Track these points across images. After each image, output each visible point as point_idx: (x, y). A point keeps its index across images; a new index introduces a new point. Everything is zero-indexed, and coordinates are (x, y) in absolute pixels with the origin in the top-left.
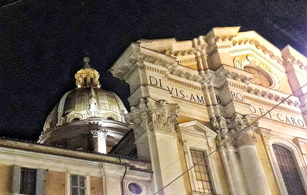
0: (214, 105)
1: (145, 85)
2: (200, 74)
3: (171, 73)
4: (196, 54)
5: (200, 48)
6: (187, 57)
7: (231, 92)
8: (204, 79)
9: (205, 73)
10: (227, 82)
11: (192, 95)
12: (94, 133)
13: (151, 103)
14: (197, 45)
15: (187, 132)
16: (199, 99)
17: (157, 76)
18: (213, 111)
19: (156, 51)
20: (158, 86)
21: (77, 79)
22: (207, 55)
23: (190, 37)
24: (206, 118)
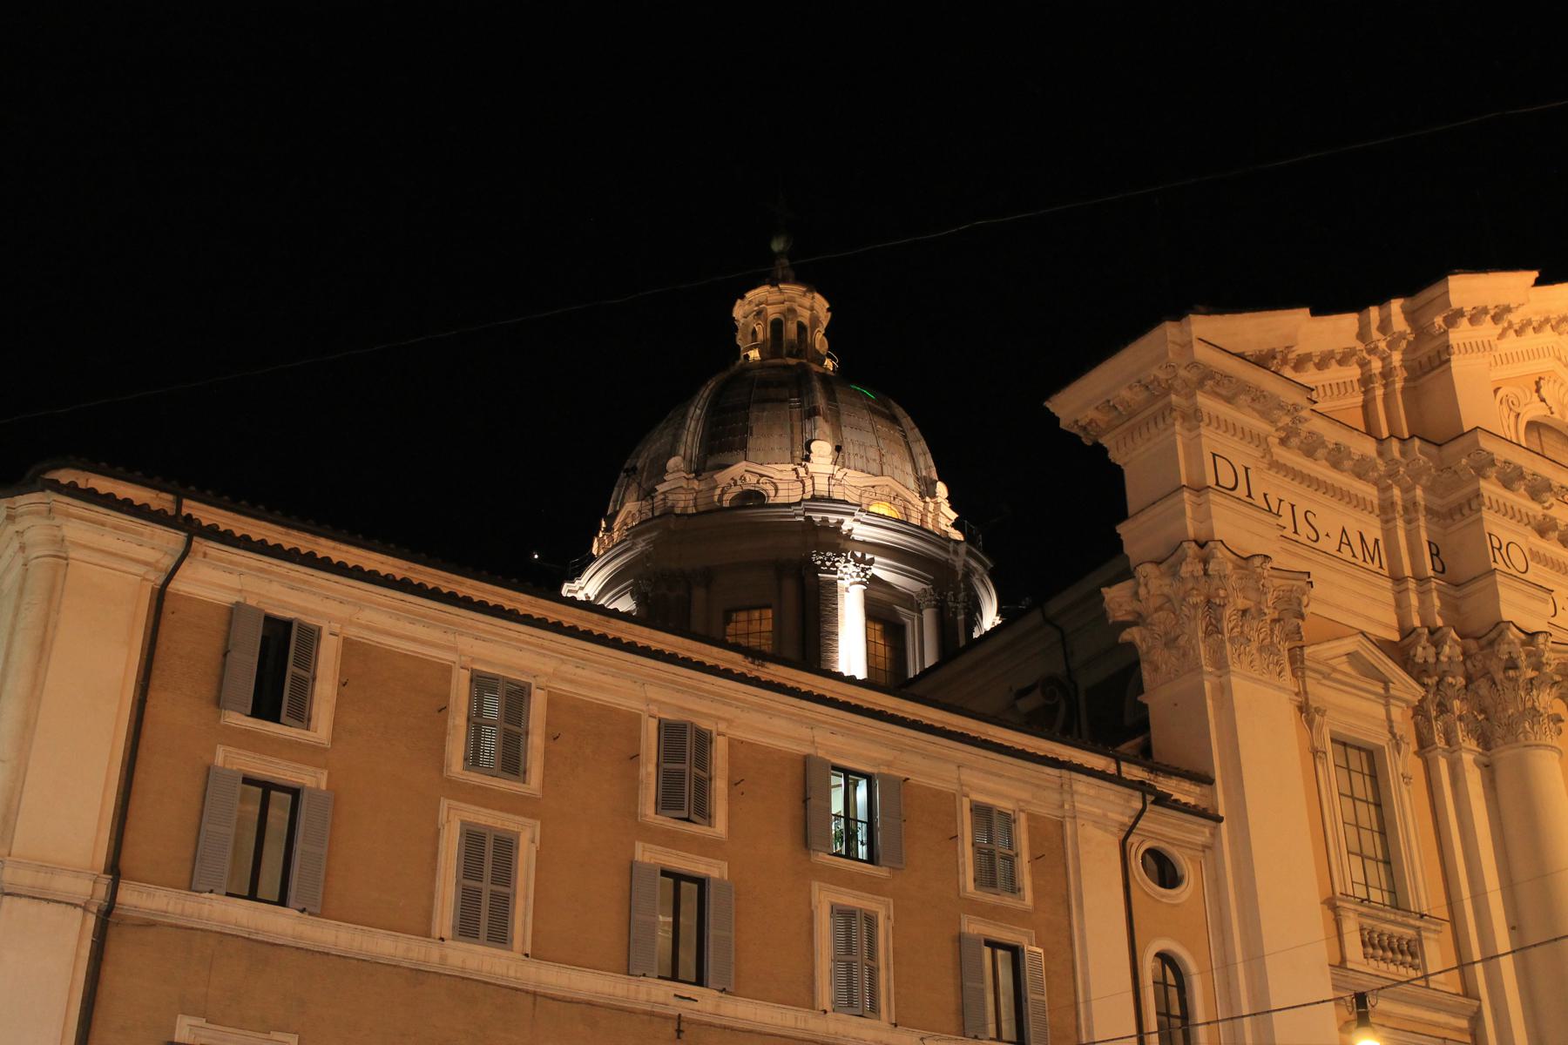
0: (1421, 580)
1: (1200, 489)
2: (1380, 454)
4: (1363, 364)
5: (1382, 345)
6: (1335, 373)
7: (1490, 535)
8: (1392, 474)
9: (1403, 454)
10: (1478, 494)
11: (1344, 530)
12: (823, 561)
13: (1222, 562)
14: (1376, 335)
15: (1326, 676)
16: (1365, 549)
17: (1239, 453)
18: (1414, 600)
19: (1241, 356)
20: (1239, 491)
21: (742, 321)
22: (1405, 375)
24: (1387, 626)
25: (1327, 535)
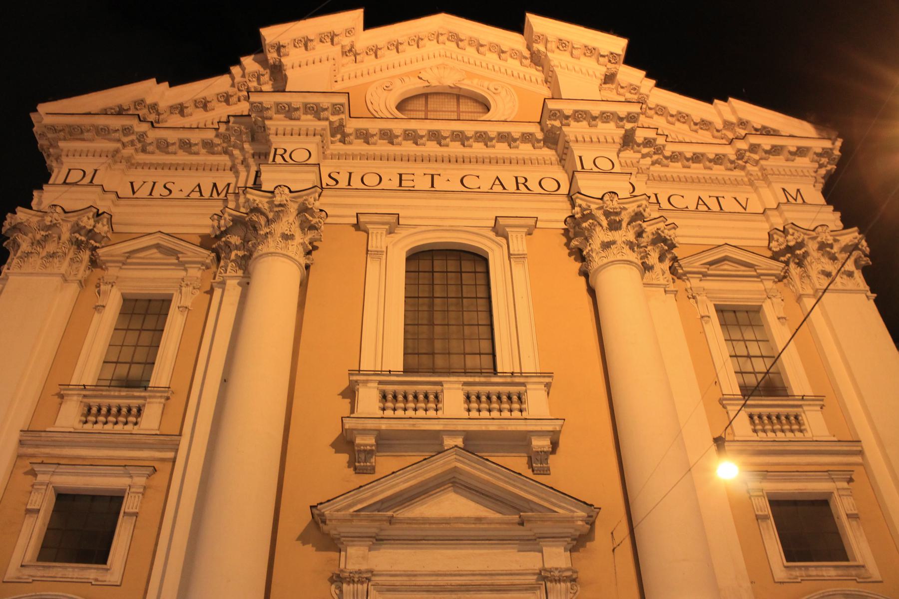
3: (144, 150)
23: (220, 68)
25: (181, 190)
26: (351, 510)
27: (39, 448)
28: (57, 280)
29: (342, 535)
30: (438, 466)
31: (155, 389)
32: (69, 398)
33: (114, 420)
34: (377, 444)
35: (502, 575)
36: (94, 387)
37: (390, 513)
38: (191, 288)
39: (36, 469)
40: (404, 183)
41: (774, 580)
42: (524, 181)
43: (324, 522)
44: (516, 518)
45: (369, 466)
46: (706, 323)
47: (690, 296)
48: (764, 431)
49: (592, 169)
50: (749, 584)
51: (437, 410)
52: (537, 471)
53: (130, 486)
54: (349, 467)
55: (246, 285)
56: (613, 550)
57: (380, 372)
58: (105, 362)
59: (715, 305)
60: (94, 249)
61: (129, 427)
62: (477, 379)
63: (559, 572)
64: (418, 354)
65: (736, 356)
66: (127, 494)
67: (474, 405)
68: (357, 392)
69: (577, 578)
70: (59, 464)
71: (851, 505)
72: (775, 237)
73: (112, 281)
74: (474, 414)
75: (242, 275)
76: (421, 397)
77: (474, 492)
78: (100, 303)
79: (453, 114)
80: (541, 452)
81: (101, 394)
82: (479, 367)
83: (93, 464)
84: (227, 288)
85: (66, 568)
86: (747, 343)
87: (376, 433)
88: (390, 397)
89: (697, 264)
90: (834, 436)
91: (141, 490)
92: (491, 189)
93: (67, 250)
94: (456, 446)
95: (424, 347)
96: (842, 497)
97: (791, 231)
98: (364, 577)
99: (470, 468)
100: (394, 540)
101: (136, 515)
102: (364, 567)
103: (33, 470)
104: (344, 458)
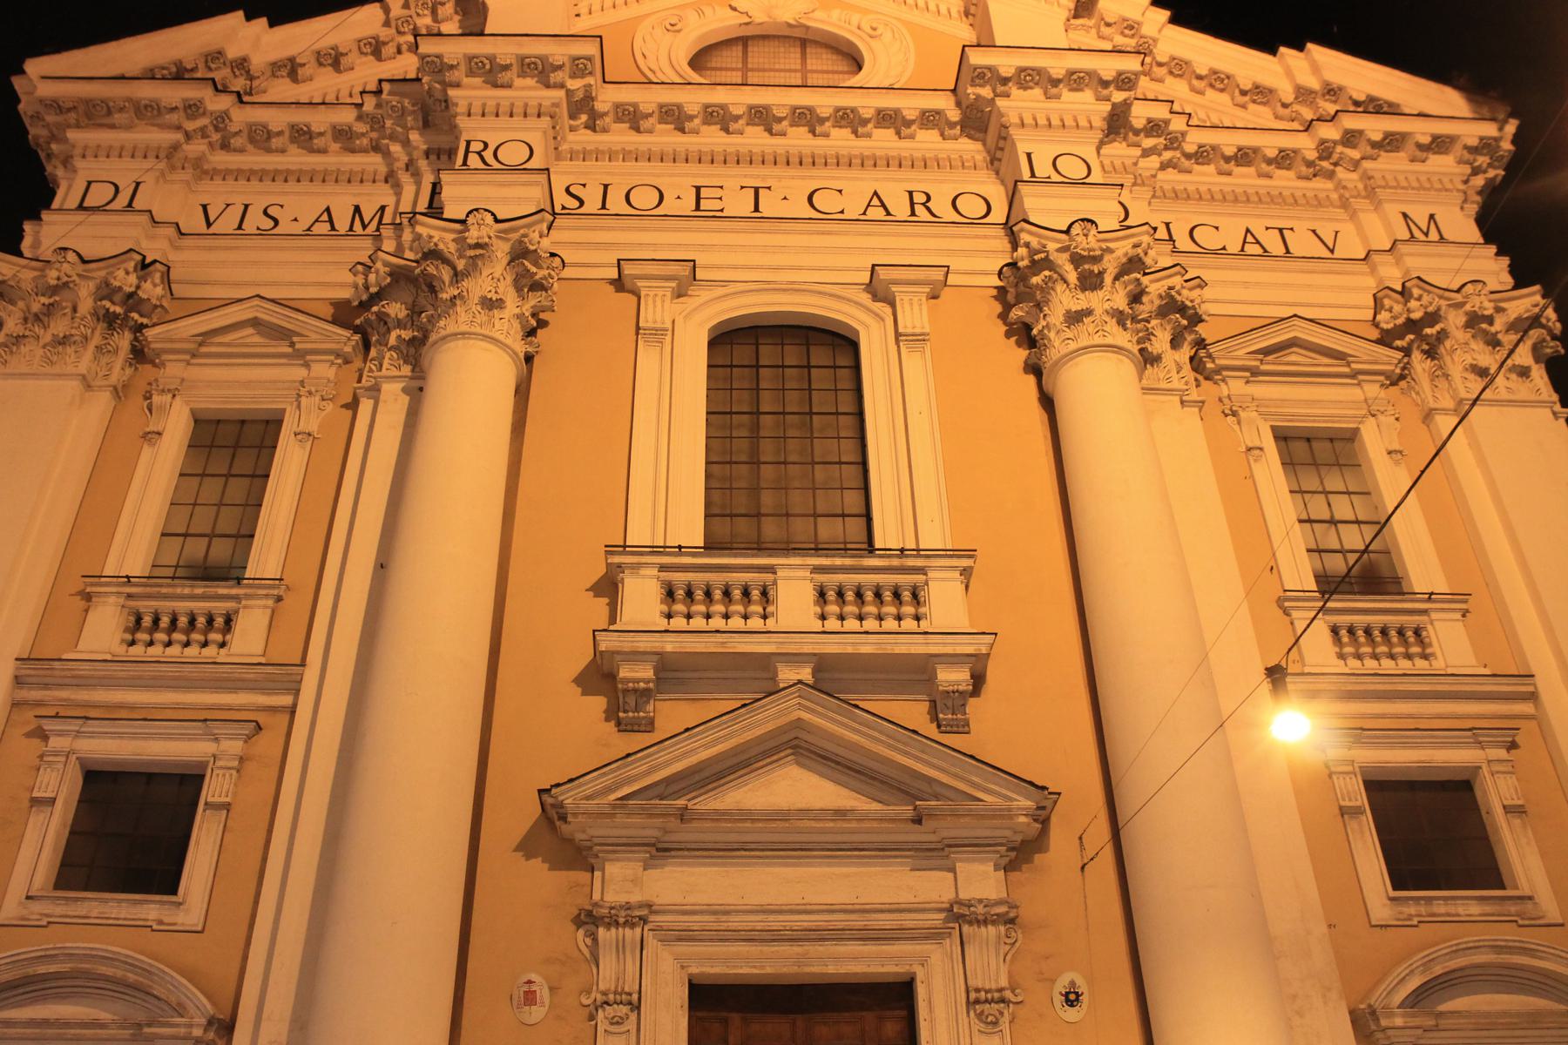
3: (225, 146)
25: (296, 220)
26: (612, 797)
27: (50, 689)
28: (74, 385)
29: (596, 840)
30: (768, 718)
31: (256, 582)
32: (102, 599)
33: (183, 638)
34: (659, 680)
35: (882, 911)
36: (145, 580)
37: (681, 802)
38: (318, 398)
39: (45, 728)
40: (704, 204)
41: (1370, 922)
42: (924, 199)
43: (563, 818)
44: (906, 810)
45: (644, 718)
46: (1255, 461)
47: (1227, 411)
48: (1359, 657)
49: (1049, 178)
50: (1324, 929)
51: (765, 617)
52: (946, 726)
53: (214, 756)
54: (607, 720)
55: (417, 393)
56: (1083, 868)
57: (662, 550)
58: (163, 535)
59: (1273, 428)
60: (140, 328)
61: (211, 651)
62: (838, 561)
63: (985, 906)
64: (731, 516)
65: (1309, 521)
66: (209, 770)
67: (833, 608)
68: (620, 585)
69: (1017, 917)
70: (87, 718)
71: (1512, 790)
72: (1387, 302)
73: (172, 387)
74: (833, 624)
75: (409, 374)
76: (737, 594)
77: (833, 765)
78: (151, 428)
79: (793, 74)
80: (953, 692)
81: (158, 593)
82: (841, 540)
83: (147, 717)
84: (382, 397)
85: (106, 901)
86: (1330, 496)
87: (656, 658)
88: (680, 593)
89: (1241, 353)
90: (1485, 666)
91: (235, 763)
92: (864, 214)
93: (89, 331)
94: (800, 682)
95: (741, 503)
96: (1496, 776)
97: (1416, 292)
98: (636, 916)
99: (826, 721)
100: (688, 850)
101: (227, 807)
102: (635, 898)
103: (40, 728)
104: (599, 703)
